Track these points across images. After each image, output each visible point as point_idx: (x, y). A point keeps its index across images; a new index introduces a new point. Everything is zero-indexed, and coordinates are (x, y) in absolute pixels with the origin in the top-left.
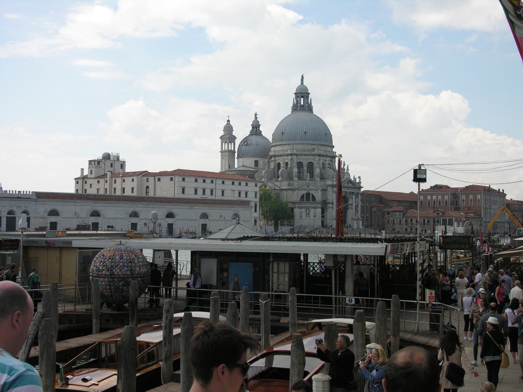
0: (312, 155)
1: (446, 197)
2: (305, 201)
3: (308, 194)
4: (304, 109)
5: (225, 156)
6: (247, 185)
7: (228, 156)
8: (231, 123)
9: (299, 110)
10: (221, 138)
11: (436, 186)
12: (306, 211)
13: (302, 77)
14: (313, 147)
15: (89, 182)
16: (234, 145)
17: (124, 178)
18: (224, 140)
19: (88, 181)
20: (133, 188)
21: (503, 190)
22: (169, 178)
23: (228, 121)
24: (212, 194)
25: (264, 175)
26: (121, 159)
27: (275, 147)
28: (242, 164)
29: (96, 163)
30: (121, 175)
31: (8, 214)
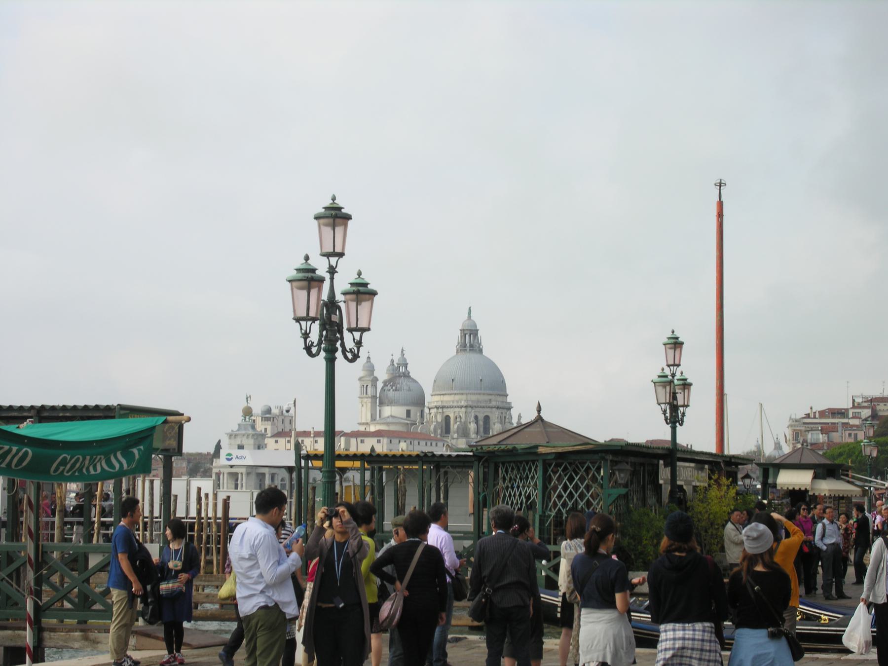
0: (489, 407)
4: (472, 350)
5: (366, 403)
6: (436, 445)
7: (370, 404)
8: (372, 360)
9: (468, 350)
13: (470, 308)
14: (490, 397)
17: (316, 439)
18: (364, 382)
21: (691, 446)
23: (369, 358)
25: (433, 430)
27: (442, 396)
28: (390, 414)
29: (272, 419)
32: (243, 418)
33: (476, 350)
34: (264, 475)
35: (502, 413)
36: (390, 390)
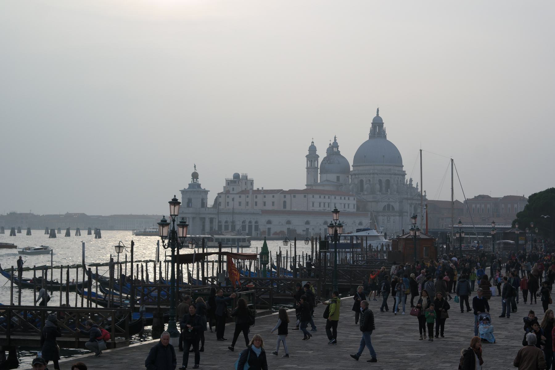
0: (389, 174)
1: (488, 206)
2: (386, 211)
3: (389, 205)
6: (349, 199)
10: (306, 157)
11: (480, 196)
12: (387, 218)
15: (231, 196)
16: (318, 162)
19: (230, 195)
20: (273, 203)
22: (303, 195)
23: (313, 142)
24: (329, 207)
26: (249, 178)
27: (358, 167)
30: (262, 193)
31: (249, 223)
32: (192, 180)
33: (382, 136)
34: (204, 218)
35: (398, 178)
36: (326, 164)
